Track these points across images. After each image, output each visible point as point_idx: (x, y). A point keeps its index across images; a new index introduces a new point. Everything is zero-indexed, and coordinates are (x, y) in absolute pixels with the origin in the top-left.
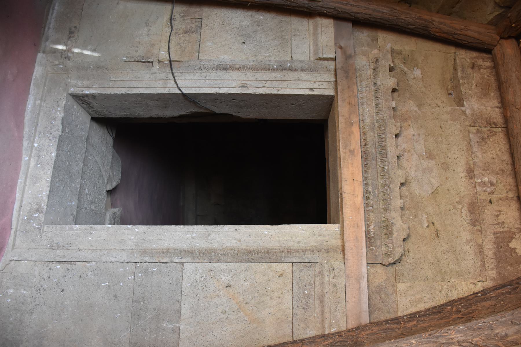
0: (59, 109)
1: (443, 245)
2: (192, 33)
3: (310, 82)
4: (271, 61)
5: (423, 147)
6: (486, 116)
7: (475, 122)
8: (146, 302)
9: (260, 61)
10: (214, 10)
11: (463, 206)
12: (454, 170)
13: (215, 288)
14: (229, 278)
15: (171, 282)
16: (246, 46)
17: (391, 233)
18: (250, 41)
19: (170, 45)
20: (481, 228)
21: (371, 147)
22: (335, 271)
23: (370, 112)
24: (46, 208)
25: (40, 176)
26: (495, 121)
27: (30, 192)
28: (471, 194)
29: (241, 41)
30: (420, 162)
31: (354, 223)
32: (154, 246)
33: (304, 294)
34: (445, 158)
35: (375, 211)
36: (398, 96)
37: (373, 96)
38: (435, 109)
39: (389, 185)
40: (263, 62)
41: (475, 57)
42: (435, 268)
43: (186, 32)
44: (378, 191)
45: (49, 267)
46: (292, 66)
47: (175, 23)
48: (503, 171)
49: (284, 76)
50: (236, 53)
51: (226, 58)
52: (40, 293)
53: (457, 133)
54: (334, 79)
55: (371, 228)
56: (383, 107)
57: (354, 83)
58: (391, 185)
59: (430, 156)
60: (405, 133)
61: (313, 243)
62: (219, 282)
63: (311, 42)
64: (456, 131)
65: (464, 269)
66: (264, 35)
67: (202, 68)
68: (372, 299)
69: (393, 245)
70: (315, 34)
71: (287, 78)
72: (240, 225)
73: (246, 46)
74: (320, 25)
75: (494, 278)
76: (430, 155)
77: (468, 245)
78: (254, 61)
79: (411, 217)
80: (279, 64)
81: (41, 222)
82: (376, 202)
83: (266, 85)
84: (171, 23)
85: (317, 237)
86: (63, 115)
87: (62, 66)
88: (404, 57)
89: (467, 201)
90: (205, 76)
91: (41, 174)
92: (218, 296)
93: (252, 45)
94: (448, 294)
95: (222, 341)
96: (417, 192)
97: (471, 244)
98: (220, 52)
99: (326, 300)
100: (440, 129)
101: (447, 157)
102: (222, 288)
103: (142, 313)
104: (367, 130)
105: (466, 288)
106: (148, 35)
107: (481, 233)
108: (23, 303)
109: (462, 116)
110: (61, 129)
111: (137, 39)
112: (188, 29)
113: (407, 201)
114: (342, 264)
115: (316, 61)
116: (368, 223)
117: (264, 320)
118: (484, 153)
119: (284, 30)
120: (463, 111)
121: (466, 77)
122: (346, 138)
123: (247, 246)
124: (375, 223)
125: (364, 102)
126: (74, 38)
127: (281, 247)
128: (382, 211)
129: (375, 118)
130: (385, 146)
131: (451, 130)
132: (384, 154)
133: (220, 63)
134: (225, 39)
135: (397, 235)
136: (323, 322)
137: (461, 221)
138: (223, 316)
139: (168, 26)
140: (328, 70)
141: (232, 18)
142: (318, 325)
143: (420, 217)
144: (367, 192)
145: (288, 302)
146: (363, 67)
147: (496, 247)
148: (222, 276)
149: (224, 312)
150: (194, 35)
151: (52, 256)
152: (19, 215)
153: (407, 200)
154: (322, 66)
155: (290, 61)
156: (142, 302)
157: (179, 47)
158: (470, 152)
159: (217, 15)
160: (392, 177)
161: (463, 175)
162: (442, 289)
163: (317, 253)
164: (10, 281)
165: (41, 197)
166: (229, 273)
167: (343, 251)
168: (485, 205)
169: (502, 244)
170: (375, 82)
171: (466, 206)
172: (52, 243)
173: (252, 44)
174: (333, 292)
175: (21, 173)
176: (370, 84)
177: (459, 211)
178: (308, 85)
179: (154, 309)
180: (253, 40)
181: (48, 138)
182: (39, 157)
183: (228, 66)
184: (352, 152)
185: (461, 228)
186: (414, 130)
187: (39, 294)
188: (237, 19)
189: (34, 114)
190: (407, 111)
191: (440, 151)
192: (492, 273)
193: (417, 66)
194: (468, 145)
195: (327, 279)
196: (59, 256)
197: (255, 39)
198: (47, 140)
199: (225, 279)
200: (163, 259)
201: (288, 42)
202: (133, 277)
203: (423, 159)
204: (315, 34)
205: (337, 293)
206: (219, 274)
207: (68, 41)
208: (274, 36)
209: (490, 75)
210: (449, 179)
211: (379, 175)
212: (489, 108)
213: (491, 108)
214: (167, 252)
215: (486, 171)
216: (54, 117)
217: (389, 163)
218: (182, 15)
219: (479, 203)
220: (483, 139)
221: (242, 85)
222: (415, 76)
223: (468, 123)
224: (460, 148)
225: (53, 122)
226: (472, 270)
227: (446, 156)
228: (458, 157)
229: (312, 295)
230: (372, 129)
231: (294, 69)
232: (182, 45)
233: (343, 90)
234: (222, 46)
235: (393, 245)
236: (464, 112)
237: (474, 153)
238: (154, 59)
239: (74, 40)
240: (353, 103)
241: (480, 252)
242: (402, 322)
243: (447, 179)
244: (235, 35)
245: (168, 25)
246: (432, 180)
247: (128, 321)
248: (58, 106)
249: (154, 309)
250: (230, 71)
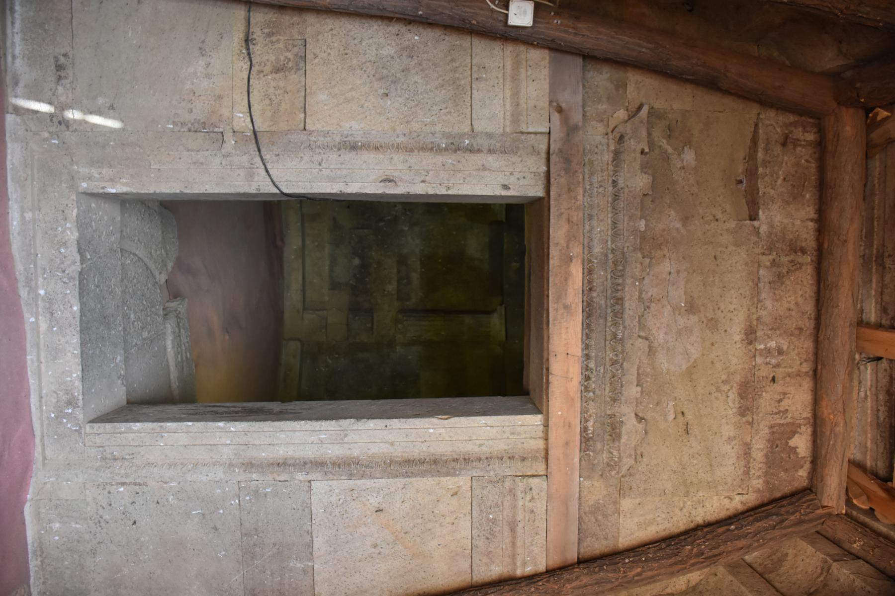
0: (68, 225)
1: (694, 445)
2: (289, 72)
3: (503, 173)
4: (436, 135)
5: (683, 293)
6: (791, 237)
7: (772, 248)
8: (261, 535)
9: (416, 134)
10: (328, 20)
11: (732, 387)
12: (726, 331)
13: (359, 514)
14: (380, 499)
15: (295, 507)
16: (389, 102)
17: (619, 436)
18: (397, 90)
19: (251, 99)
20: (753, 419)
21: (598, 295)
22: (533, 491)
23: (602, 233)
24: (83, 399)
25: (61, 346)
26: (804, 244)
27: (50, 373)
28: (745, 368)
29: (379, 91)
30: (675, 318)
31: (564, 422)
32: (263, 454)
33: (487, 519)
34: (714, 310)
35: (597, 399)
36: (652, 201)
37: (609, 205)
38: (710, 225)
39: (622, 364)
40: (421, 137)
41: (791, 124)
42: (677, 478)
43: (278, 70)
44: (604, 368)
45: (107, 490)
46: (472, 145)
47: (256, 49)
48: (801, 329)
49: (459, 161)
50: (372, 118)
51: (355, 128)
52: (101, 526)
53: (740, 268)
54: (545, 168)
55: (590, 424)
56: (625, 229)
57: (579, 183)
58: (625, 364)
59: (692, 308)
60: (655, 269)
61: (501, 446)
62: (365, 505)
63: (508, 94)
64: (738, 264)
65: (719, 479)
66: (422, 77)
67: (313, 147)
68: (584, 523)
69: (620, 454)
70: (515, 79)
71: (464, 166)
72: (392, 420)
73: (389, 102)
74: (524, 63)
75: (759, 489)
76: (692, 307)
77: (730, 444)
78: (404, 135)
79: (651, 406)
80: (450, 141)
81: (79, 421)
82: (600, 385)
83: (427, 178)
84: (248, 49)
85: (509, 435)
86: (77, 234)
87: (57, 142)
88: (669, 125)
89: (739, 379)
90: (320, 161)
91: (61, 342)
92: (365, 524)
93: (400, 100)
94: (692, 512)
95: (374, 583)
96: (665, 366)
97: (734, 442)
98: (344, 114)
99: (519, 529)
100: (712, 261)
101: (719, 309)
102: (370, 514)
103: (257, 549)
104: (596, 265)
105: (718, 505)
106: (208, 76)
107: (752, 427)
108: (78, 541)
109: (752, 237)
110: (79, 261)
111: (188, 85)
112: (281, 63)
113: (647, 382)
114: (543, 482)
115: (515, 134)
116: (586, 415)
117: (431, 554)
118: (777, 300)
119: (459, 67)
120: (755, 228)
121: (770, 162)
122: (559, 284)
123: (404, 452)
124: (596, 417)
125: (594, 214)
126: (68, 81)
127: (455, 452)
128: (608, 399)
129: (609, 246)
130: (622, 299)
131: (730, 262)
132: (618, 312)
133: (345, 139)
134: (350, 86)
135: (627, 440)
136: (514, 556)
137: (725, 409)
138: (374, 550)
139: (243, 55)
140: (535, 151)
141: (362, 39)
142: (507, 560)
143: (665, 405)
144: (587, 368)
145: (465, 529)
146: (597, 147)
147: (769, 446)
148: (369, 497)
149: (375, 546)
150: (293, 77)
151: (109, 475)
152: (42, 411)
153: (648, 379)
154: (526, 145)
155: (470, 135)
156: (255, 535)
157: (267, 101)
158: (755, 300)
159: (334, 32)
160: (627, 351)
161: (737, 338)
162: (684, 507)
163: (508, 461)
164: (51, 512)
165: (71, 381)
166: (378, 492)
167: (547, 459)
168: (764, 385)
169: (778, 442)
170: (615, 179)
171: (735, 388)
172: (104, 453)
173: (400, 96)
174: (529, 521)
175: (28, 346)
176: (606, 181)
177: (724, 395)
178: (499, 179)
179: (274, 545)
180: (402, 89)
181: (60, 279)
182: (52, 314)
183: (360, 144)
184: (567, 307)
185: (724, 420)
186: (671, 265)
187: (99, 528)
188: (371, 41)
189: (26, 238)
190: (664, 230)
191: (709, 299)
192: (757, 483)
193: (688, 143)
194: (754, 288)
195: (521, 503)
196: (119, 474)
197: (405, 87)
198: (60, 284)
199: (374, 501)
200: (279, 475)
201: (465, 94)
202: (237, 501)
203: (679, 315)
204: (515, 79)
205: (534, 521)
206: (365, 495)
207: (58, 86)
208: (440, 81)
209: (810, 159)
210: (716, 346)
211: (608, 343)
212: (798, 222)
213: (801, 221)
214: (282, 464)
215: (775, 330)
216: (64, 241)
217: (625, 327)
218: (266, 31)
219: (756, 382)
220: (780, 277)
221: (386, 177)
222: (685, 162)
223: (758, 250)
224: (741, 294)
225: (63, 250)
226: (729, 480)
227: (717, 307)
228: (734, 309)
229: (499, 520)
230: (604, 264)
231: (476, 149)
232: (273, 97)
233: (559, 196)
234: (347, 101)
235: (620, 454)
236: (757, 231)
237: (762, 302)
238: (224, 128)
239: (69, 85)
240: (575, 219)
241: (745, 454)
242: (622, 569)
243: (713, 344)
244: (368, 77)
245: (243, 53)
246: (689, 347)
247: (238, 561)
248: (66, 219)
249: (274, 545)
250: (363, 152)
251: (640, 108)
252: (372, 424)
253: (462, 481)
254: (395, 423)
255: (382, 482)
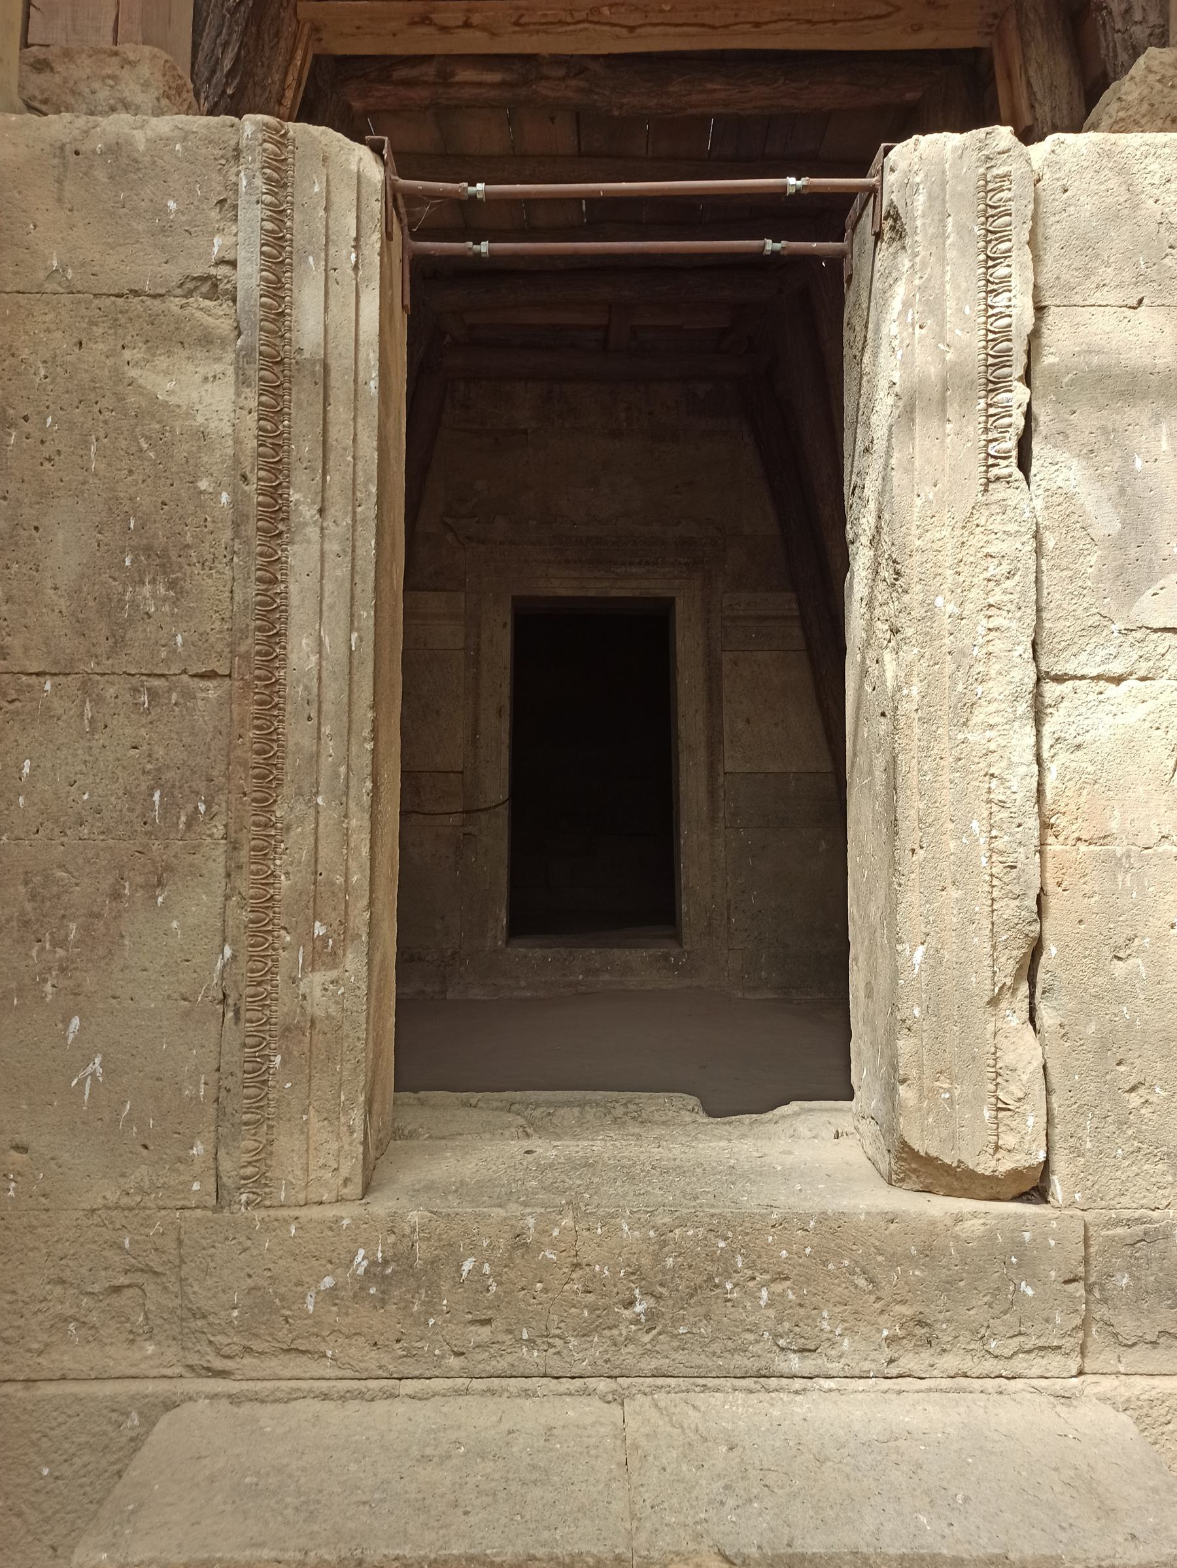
55: (682, 560)
195: (741, 613)
214: (712, 793)
251: (446, 524)
252: (681, 727)
253: (726, 657)
254: (681, 709)
255: (726, 718)
